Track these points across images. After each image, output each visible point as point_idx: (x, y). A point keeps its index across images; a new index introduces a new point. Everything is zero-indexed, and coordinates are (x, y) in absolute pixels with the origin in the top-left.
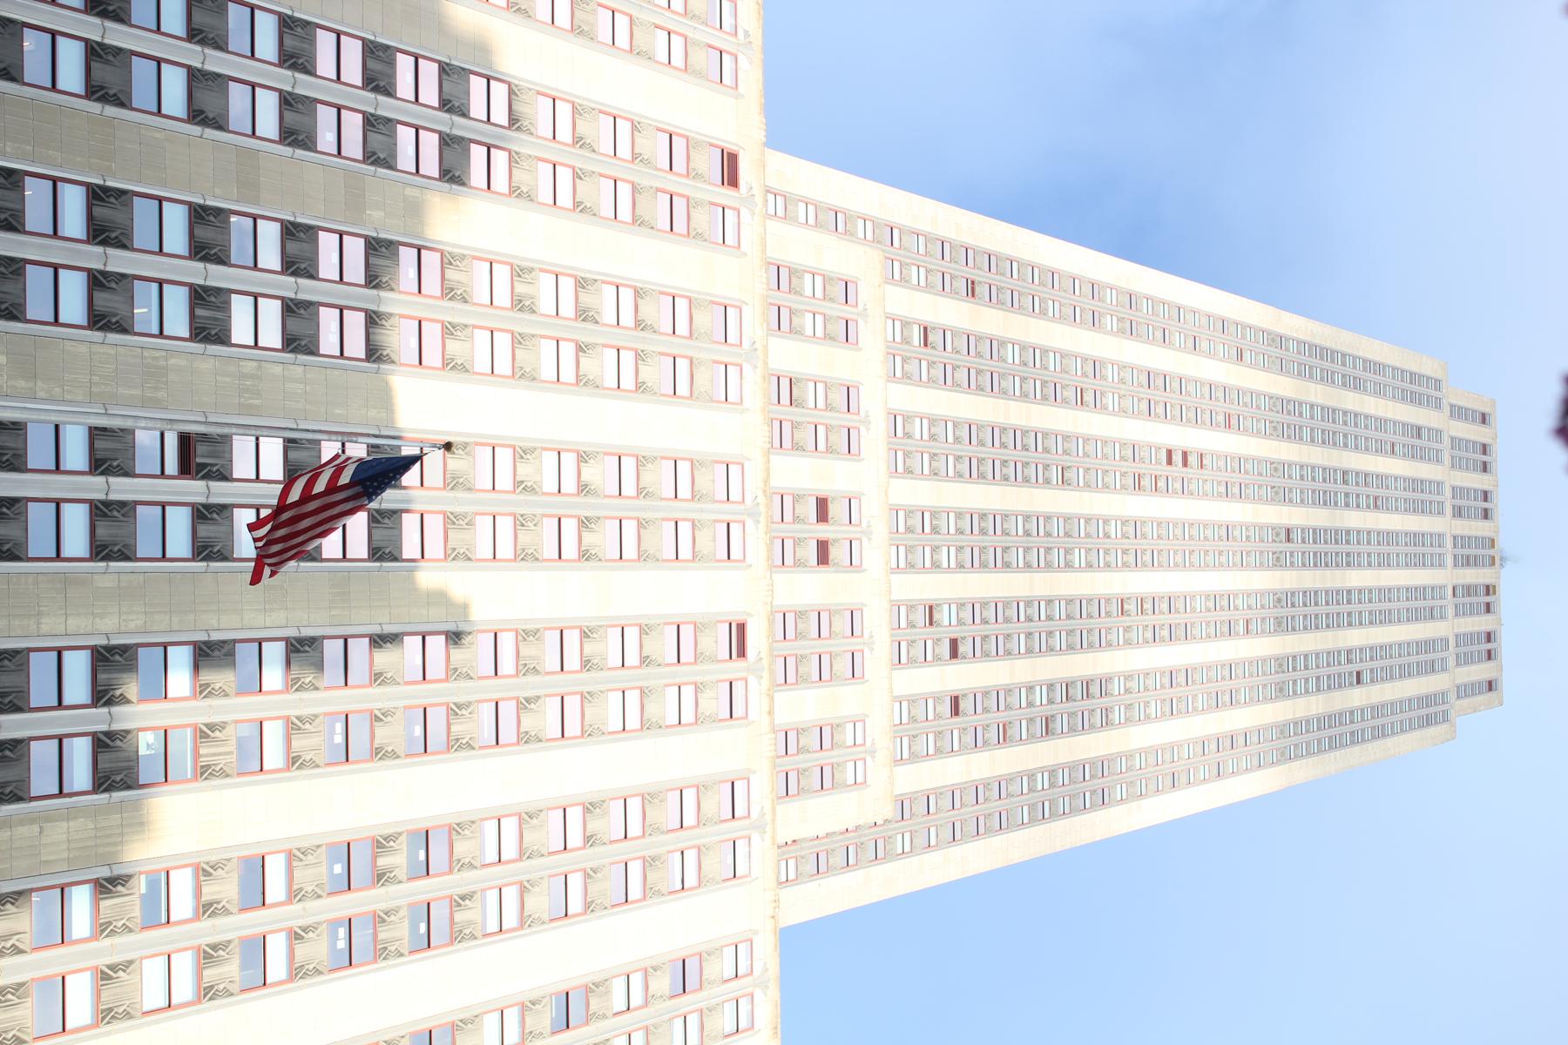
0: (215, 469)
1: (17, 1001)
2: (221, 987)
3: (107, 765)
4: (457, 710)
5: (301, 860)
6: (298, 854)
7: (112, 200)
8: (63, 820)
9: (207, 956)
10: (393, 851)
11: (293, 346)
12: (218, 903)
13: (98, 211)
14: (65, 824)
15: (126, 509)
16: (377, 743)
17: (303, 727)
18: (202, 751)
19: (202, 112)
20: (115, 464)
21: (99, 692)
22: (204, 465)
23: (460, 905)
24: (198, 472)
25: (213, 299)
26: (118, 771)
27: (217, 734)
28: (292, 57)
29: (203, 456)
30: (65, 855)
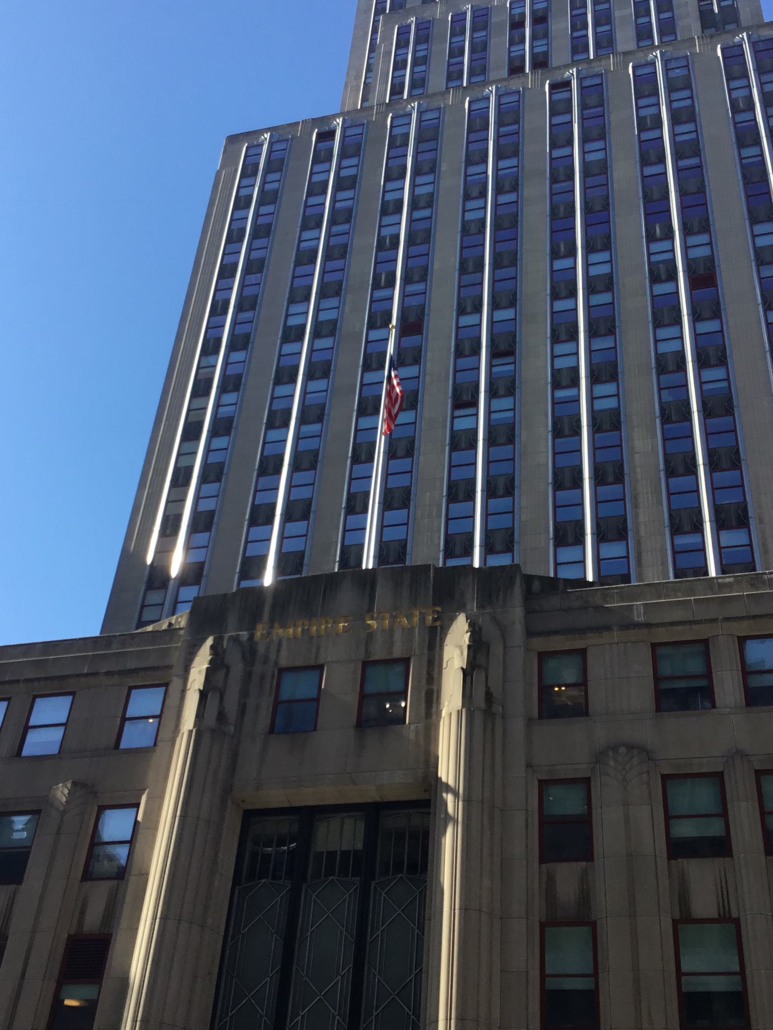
1: (717, 456)
27: (596, 373)
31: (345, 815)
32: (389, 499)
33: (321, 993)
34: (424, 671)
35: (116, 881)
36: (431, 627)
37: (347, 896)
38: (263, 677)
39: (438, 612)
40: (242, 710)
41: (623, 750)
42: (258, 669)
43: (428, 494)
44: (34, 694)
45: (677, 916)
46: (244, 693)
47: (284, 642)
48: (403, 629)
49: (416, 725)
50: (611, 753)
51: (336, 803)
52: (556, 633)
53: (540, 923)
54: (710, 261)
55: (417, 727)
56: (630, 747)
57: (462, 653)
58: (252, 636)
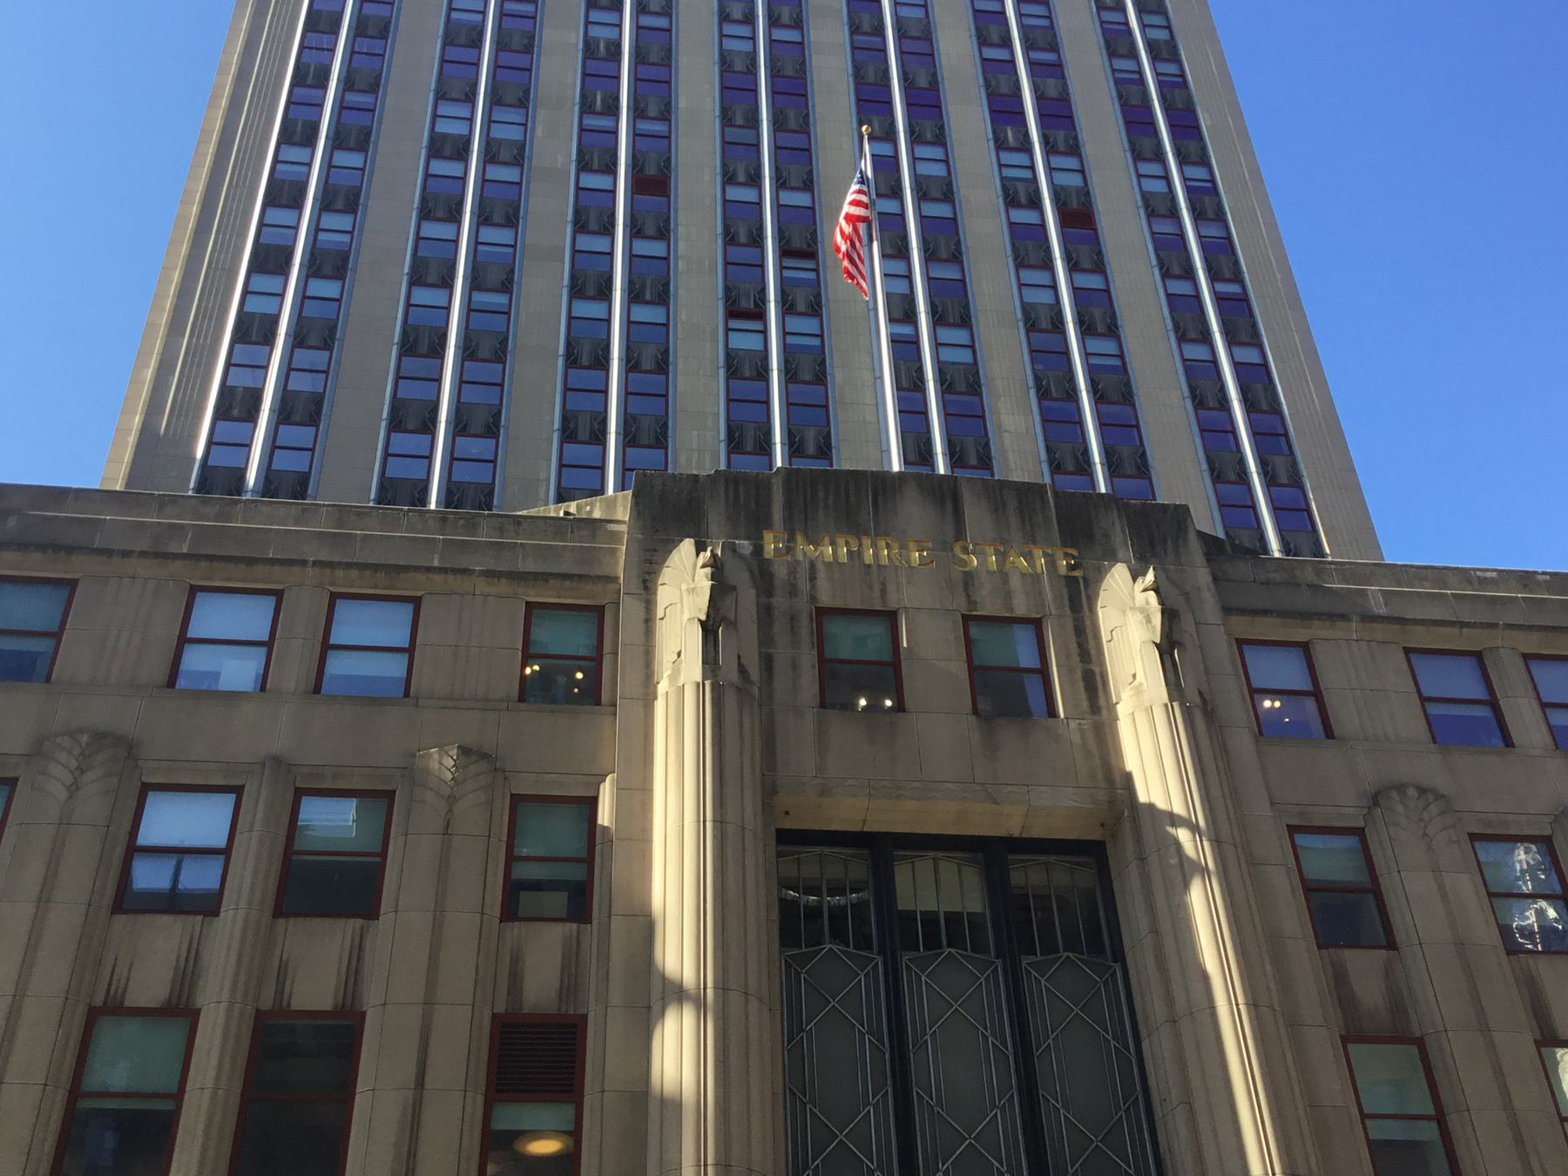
0: (757, 296)
2: (1109, 321)
3: (964, 385)
4: (916, 135)
5: (1023, 258)
6: (1019, 259)
7: (576, 351)
8: (999, 417)
9: (1088, 329)
10: (1016, 191)
11: (665, 232)
12: (1052, 317)
13: (585, 362)
14: (1002, 416)
15: (790, 359)
16: (940, 196)
17: (932, 248)
18: (952, 321)
19: (503, 283)
20: (759, 364)
21: (915, 387)
22: (755, 301)
23: (1053, 146)
24: (761, 308)
25: (637, 287)
26: (967, 378)
28: (451, 213)
29: (750, 304)
30: (1022, 417)
31: (940, 854)
32: (633, 429)
33: (970, 1135)
34: (1073, 646)
35: (575, 926)
36: (1067, 577)
37: (983, 980)
38: (793, 618)
39: (1073, 557)
40: (768, 662)
41: (1411, 792)
42: (780, 601)
43: (695, 433)
44: (333, 589)
45: (1538, 1037)
46: (766, 639)
47: (820, 567)
48: (1023, 575)
49: (1078, 721)
50: (1395, 795)
51: (941, 833)
52: (1266, 612)
53: (1341, 1036)
54: (1085, 193)
55: (1080, 724)
56: (1422, 791)
57: (1148, 620)
58: (758, 550)
